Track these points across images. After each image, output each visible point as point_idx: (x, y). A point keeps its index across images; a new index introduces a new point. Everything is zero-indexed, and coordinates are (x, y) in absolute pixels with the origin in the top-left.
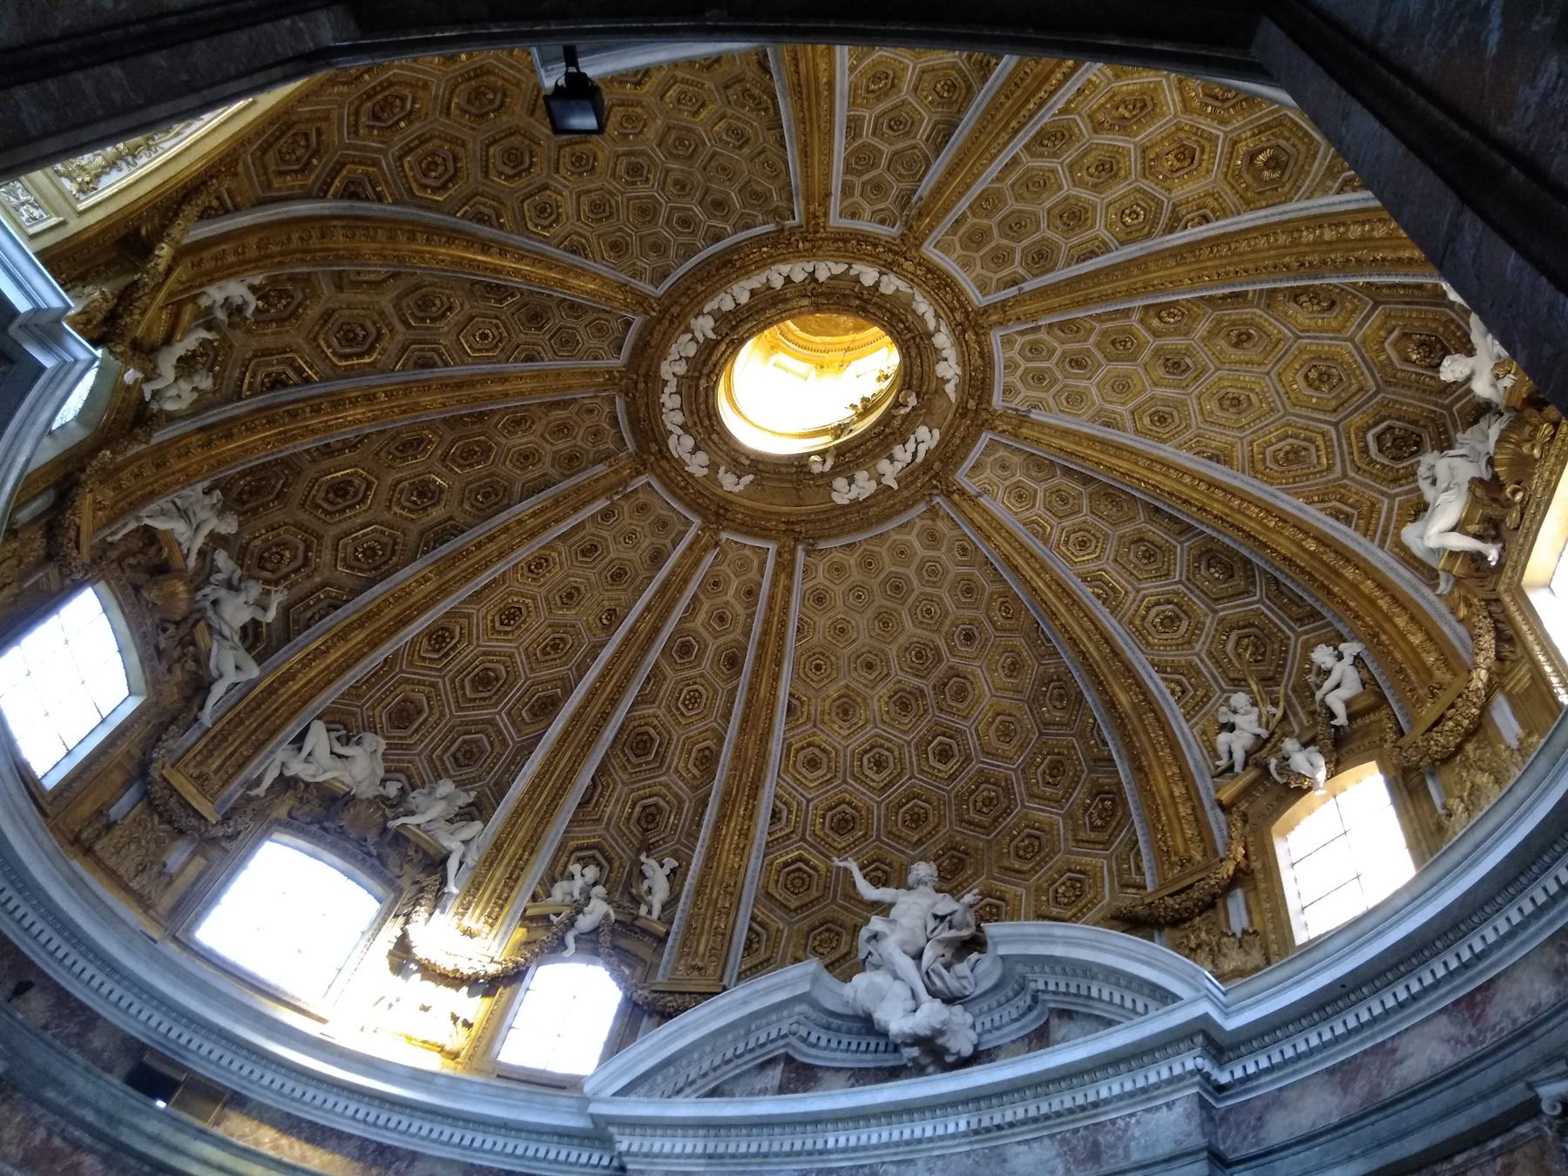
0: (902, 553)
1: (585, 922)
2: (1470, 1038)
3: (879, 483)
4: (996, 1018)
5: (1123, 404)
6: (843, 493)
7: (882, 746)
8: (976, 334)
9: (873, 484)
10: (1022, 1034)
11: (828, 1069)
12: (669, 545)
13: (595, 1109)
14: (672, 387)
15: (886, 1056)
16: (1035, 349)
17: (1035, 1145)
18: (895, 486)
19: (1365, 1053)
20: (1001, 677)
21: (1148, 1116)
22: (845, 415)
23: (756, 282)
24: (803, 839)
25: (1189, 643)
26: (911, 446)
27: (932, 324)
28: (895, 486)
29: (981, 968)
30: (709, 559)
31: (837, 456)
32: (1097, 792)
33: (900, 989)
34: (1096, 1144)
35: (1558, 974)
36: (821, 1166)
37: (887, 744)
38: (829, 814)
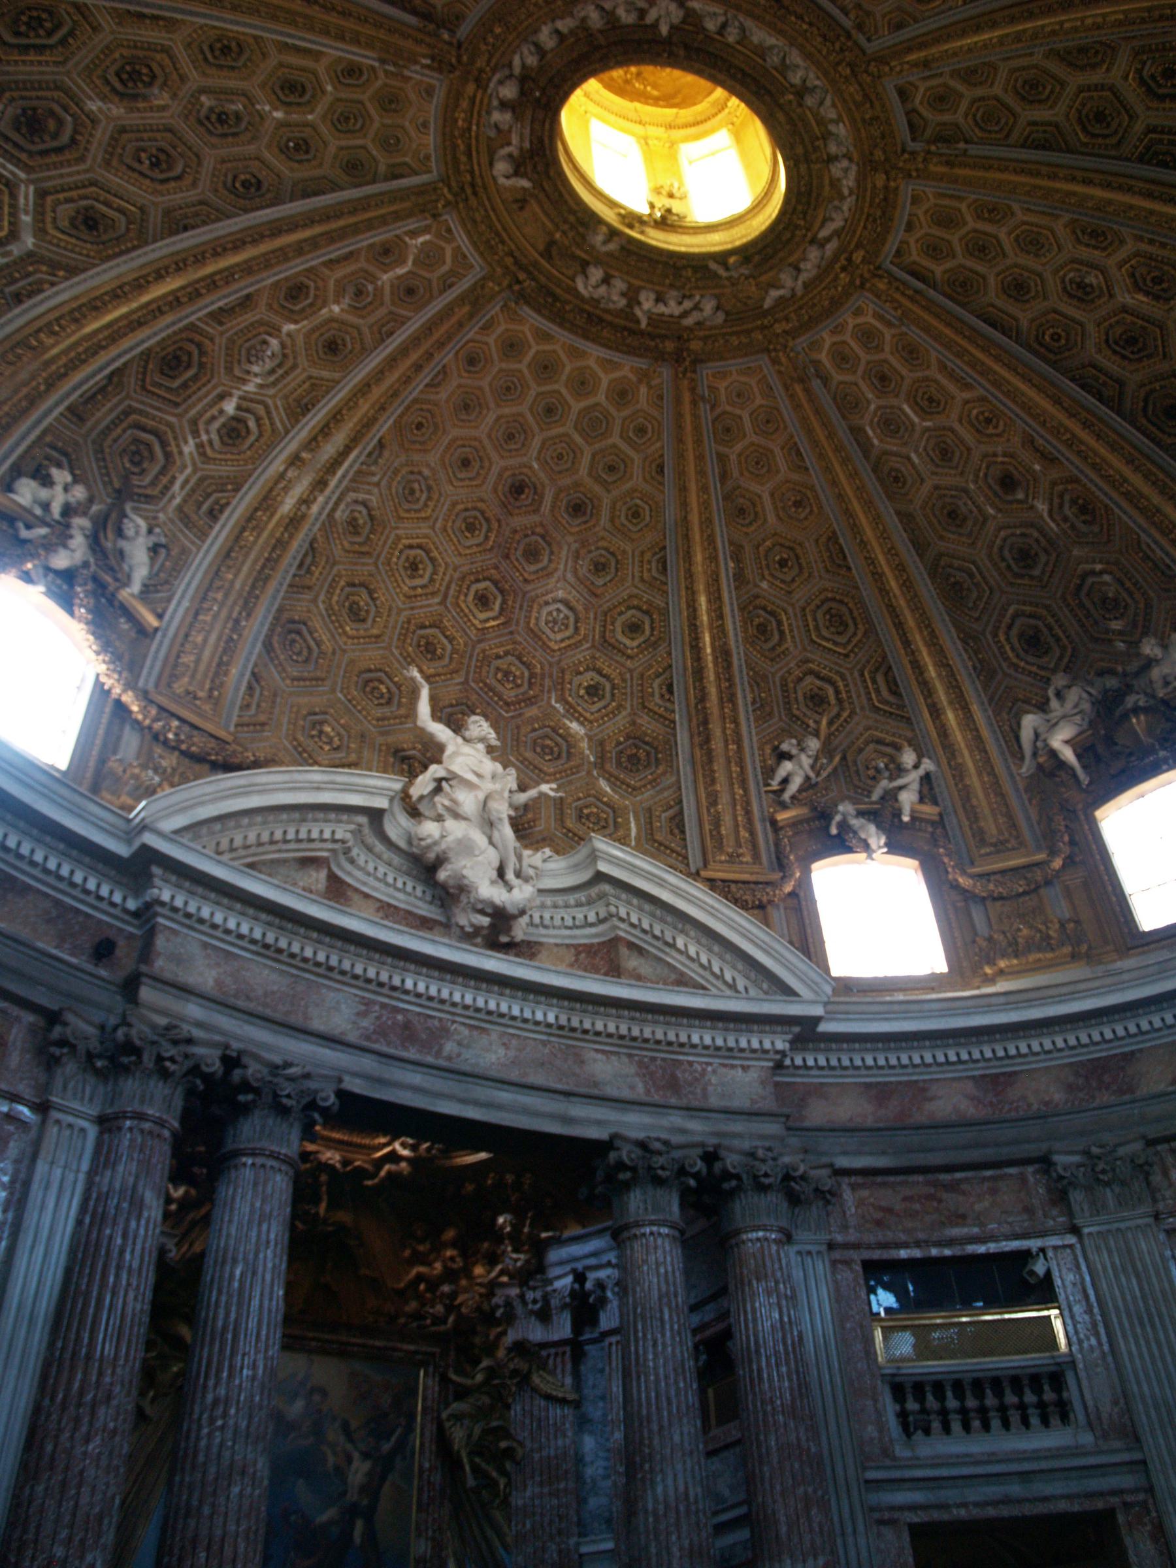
0: (582, 384)
1: (61, 561)
2: (991, 1104)
3: (630, 306)
4: (547, 916)
5: (881, 441)
6: (589, 284)
7: (427, 552)
8: (852, 282)
9: (623, 302)
10: (568, 941)
11: (356, 890)
12: (382, 168)
13: (149, 839)
14: (565, 25)
15: (420, 903)
16: (867, 336)
17: (613, 1058)
18: (644, 324)
19: (900, 1083)
20: (584, 567)
21: (724, 1070)
22: (644, 210)
23: (760, 35)
24: (314, 601)
25: (772, 660)
26: (687, 304)
27: (823, 234)
28: (644, 324)
29: (551, 865)
30: (412, 223)
31: (623, 248)
32: (635, 737)
33: (492, 857)
34: (673, 1076)
35: (1070, 1088)
36: (386, 1000)
37: (435, 554)
38: (348, 589)
